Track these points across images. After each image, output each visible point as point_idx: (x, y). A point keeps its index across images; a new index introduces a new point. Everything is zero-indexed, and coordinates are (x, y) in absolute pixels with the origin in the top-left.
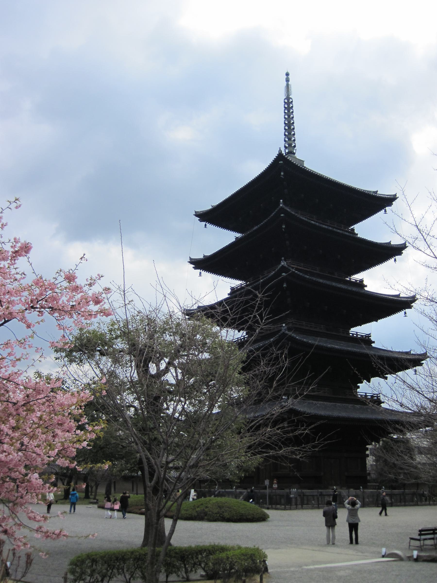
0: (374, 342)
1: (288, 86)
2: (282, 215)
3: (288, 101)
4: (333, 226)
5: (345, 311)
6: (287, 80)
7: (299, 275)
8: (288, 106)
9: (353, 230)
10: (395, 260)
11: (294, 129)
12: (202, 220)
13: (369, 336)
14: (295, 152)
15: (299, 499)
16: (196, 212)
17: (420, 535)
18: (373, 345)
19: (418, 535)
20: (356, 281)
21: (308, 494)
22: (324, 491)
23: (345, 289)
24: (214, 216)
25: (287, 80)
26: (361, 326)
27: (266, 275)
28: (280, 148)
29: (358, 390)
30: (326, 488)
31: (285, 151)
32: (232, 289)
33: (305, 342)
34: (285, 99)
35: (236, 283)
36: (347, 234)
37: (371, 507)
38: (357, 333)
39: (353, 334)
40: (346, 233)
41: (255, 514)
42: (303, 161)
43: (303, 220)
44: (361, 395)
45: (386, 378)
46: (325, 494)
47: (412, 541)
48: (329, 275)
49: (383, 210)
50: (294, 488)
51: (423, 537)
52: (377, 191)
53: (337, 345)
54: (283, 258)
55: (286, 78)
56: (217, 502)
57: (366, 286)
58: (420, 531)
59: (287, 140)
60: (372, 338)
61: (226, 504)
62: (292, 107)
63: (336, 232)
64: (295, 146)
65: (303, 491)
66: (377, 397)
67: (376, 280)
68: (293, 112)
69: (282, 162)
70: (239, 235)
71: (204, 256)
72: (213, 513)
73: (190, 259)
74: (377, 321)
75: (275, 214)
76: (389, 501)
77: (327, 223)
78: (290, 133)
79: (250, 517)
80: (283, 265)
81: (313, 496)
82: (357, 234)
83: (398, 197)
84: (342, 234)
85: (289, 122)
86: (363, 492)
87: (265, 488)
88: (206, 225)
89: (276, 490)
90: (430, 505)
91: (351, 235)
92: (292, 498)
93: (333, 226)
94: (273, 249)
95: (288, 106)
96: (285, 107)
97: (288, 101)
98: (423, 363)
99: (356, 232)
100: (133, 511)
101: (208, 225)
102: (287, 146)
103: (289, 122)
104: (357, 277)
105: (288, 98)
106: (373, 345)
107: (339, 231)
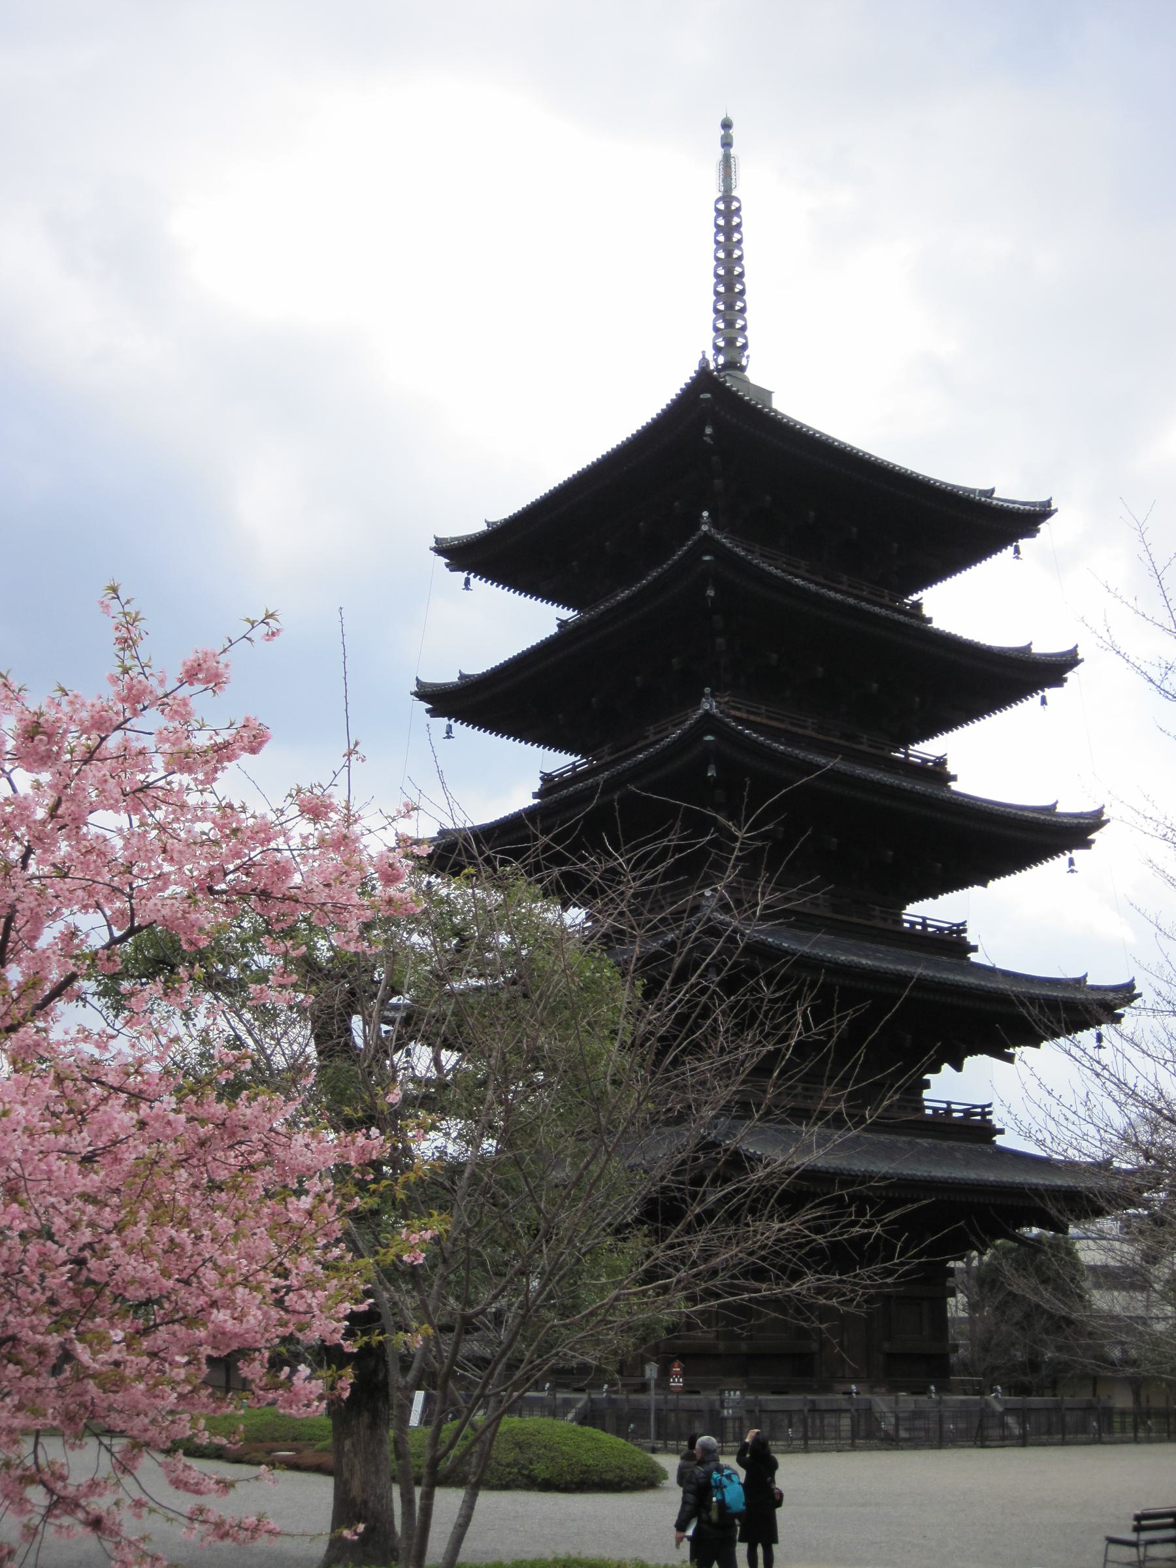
0: (975, 949)
2: (707, 558)
3: (728, 206)
4: (855, 592)
5: (891, 853)
6: (727, 143)
7: (755, 741)
8: (728, 221)
9: (917, 606)
10: (1044, 701)
11: (742, 292)
12: (455, 566)
13: (960, 928)
14: (744, 362)
16: (437, 540)
17: (1138, 1529)
18: (973, 957)
19: (1131, 1528)
20: (925, 761)
21: (772, 1407)
22: (822, 1400)
23: (892, 787)
24: (497, 554)
25: (727, 143)
26: (935, 897)
27: (652, 738)
28: (704, 353)
29: (926, 1094)
30: (826, 1388)
31: (716, 360)
32: (547, 778)
33: (770, 946)
34: (717, 201)
35: (559, 761)
36: (902, 618)
37: (963, 1447)
38: (924, 919)
39: (913, 924)
40: (897, 616)
41: (626, 1467)
42: (770, 393)
43: (770, 574)
44: (935, 1110)
45: (1010, 1058)
46: (824, 1407)
47: (1114, 1548)
48: (842, 742)
49: (1011, 549)
50: (735, 1390)
51: (1146, 1536)
52: (993, 491)
53: (867, 957)
54: (707, 690)
55: (722, 138)
56: (511, 1431)
57: (954, 778)
58: (1138, 1518)
59: (721, 325)
60: (971, 937)
61: (539, 1437)
62: (739, 225)
63: (869, 612)
64: (745, 347)
65: (760, 1397)
66: (984, 1114)
67: (984, 758)
68: (740, 241)
69: (708, 396)
70: (568, 614)
71: (462, 676)
72: (499, 1464)
74: (985, 885)
75: (687, 553)
76: (1017, 1431)
77: (841, 583)
78: (730, 306)
79: (609, 1476)
80: (707, 714)
81: (789, 1413)
82: (930, 620)
83: (1056, 510)
84: (886, 618)
85: (729, 271)
86: (940, 1402)
87: (644, 1388)
89: (678, 1393)
90: (1136, 1441)
91: (914, 622)
92: (726, 1419)
93: (855, 592)
94: (675, 661)
95: (728, 221)
96: (717, 226)
97: (728, 206)
98: (1122, 1016)
99: (927, 611)
100: (247, 1457)
101: (475, 581)
102: (722, 344)
103: (729, 271)
104: (927, 749)
105: (727, 197)
106: (973, 957)
107: (877, 609)
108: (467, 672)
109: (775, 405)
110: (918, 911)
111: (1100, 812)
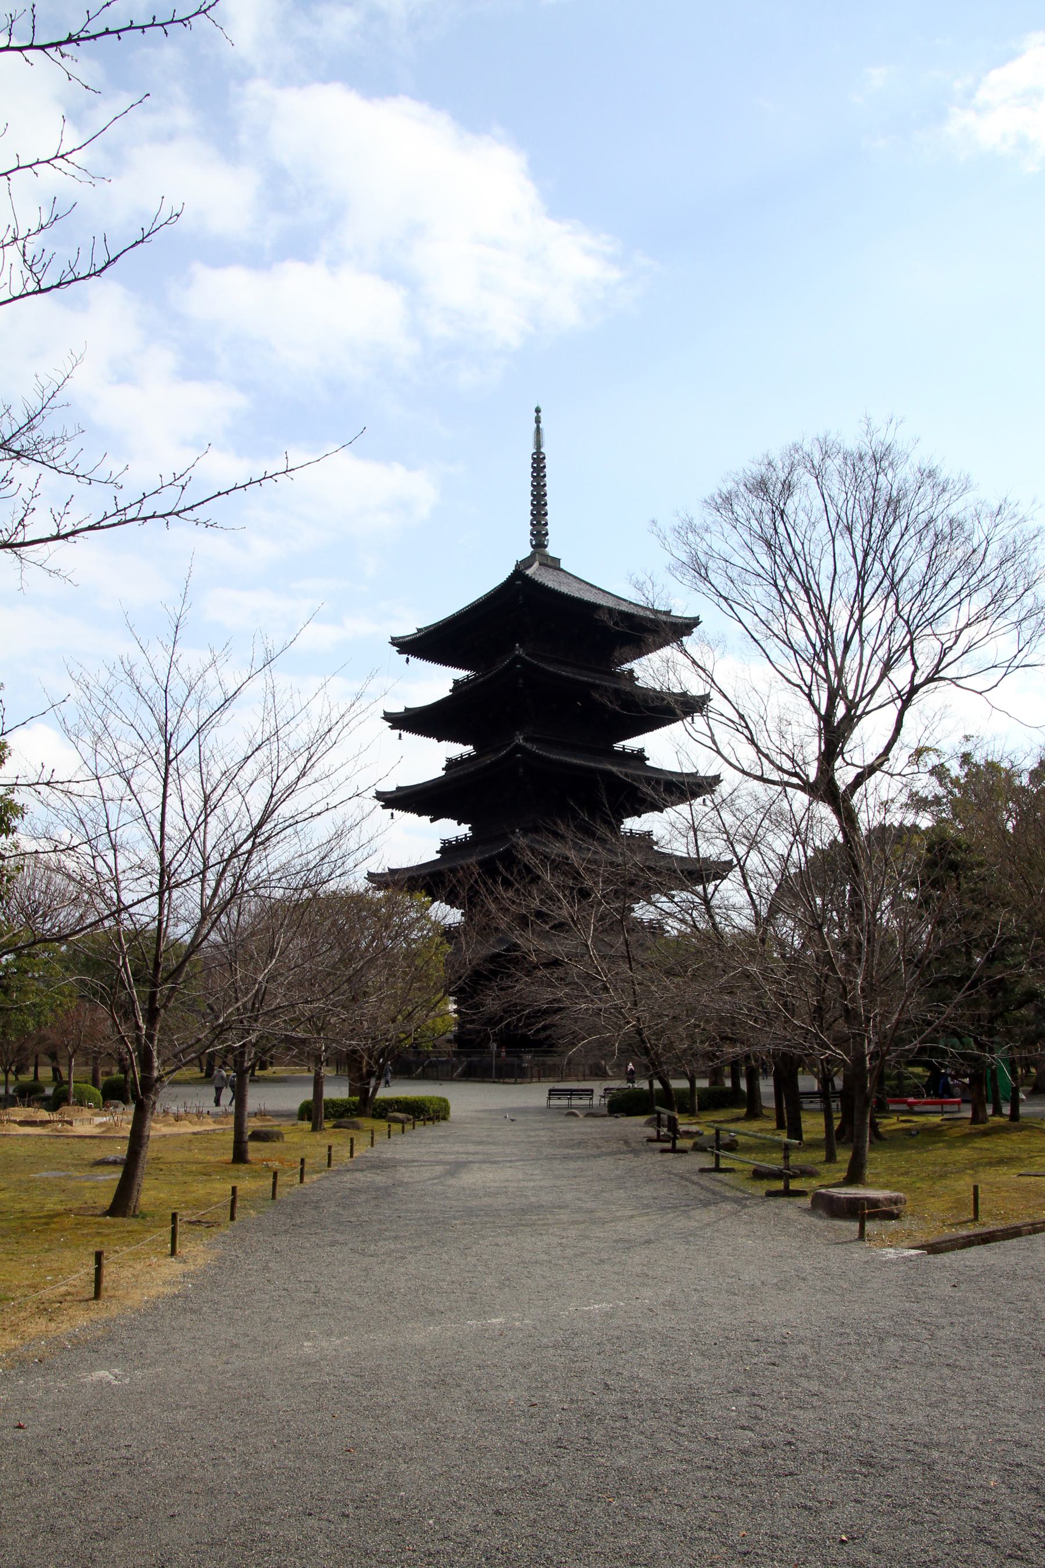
1: (538, 431)
6: (538, 421)
7: (541, 755)
9: (631, 671)
15: (536, 1069)
16: (392, 638)
25: (538, 421)
35: (458, 750)
62: (544, 467)
64: (547, 534)
70: (461, 674)
71: (406, 709)
73: (385, 713)
88: (408, 660)
101: (412, 659)
103: (538, 493)
104: (632, 744)
108: (409, 706)
109: (562, 566)
110: (632, 824)
111: (719, 776)
